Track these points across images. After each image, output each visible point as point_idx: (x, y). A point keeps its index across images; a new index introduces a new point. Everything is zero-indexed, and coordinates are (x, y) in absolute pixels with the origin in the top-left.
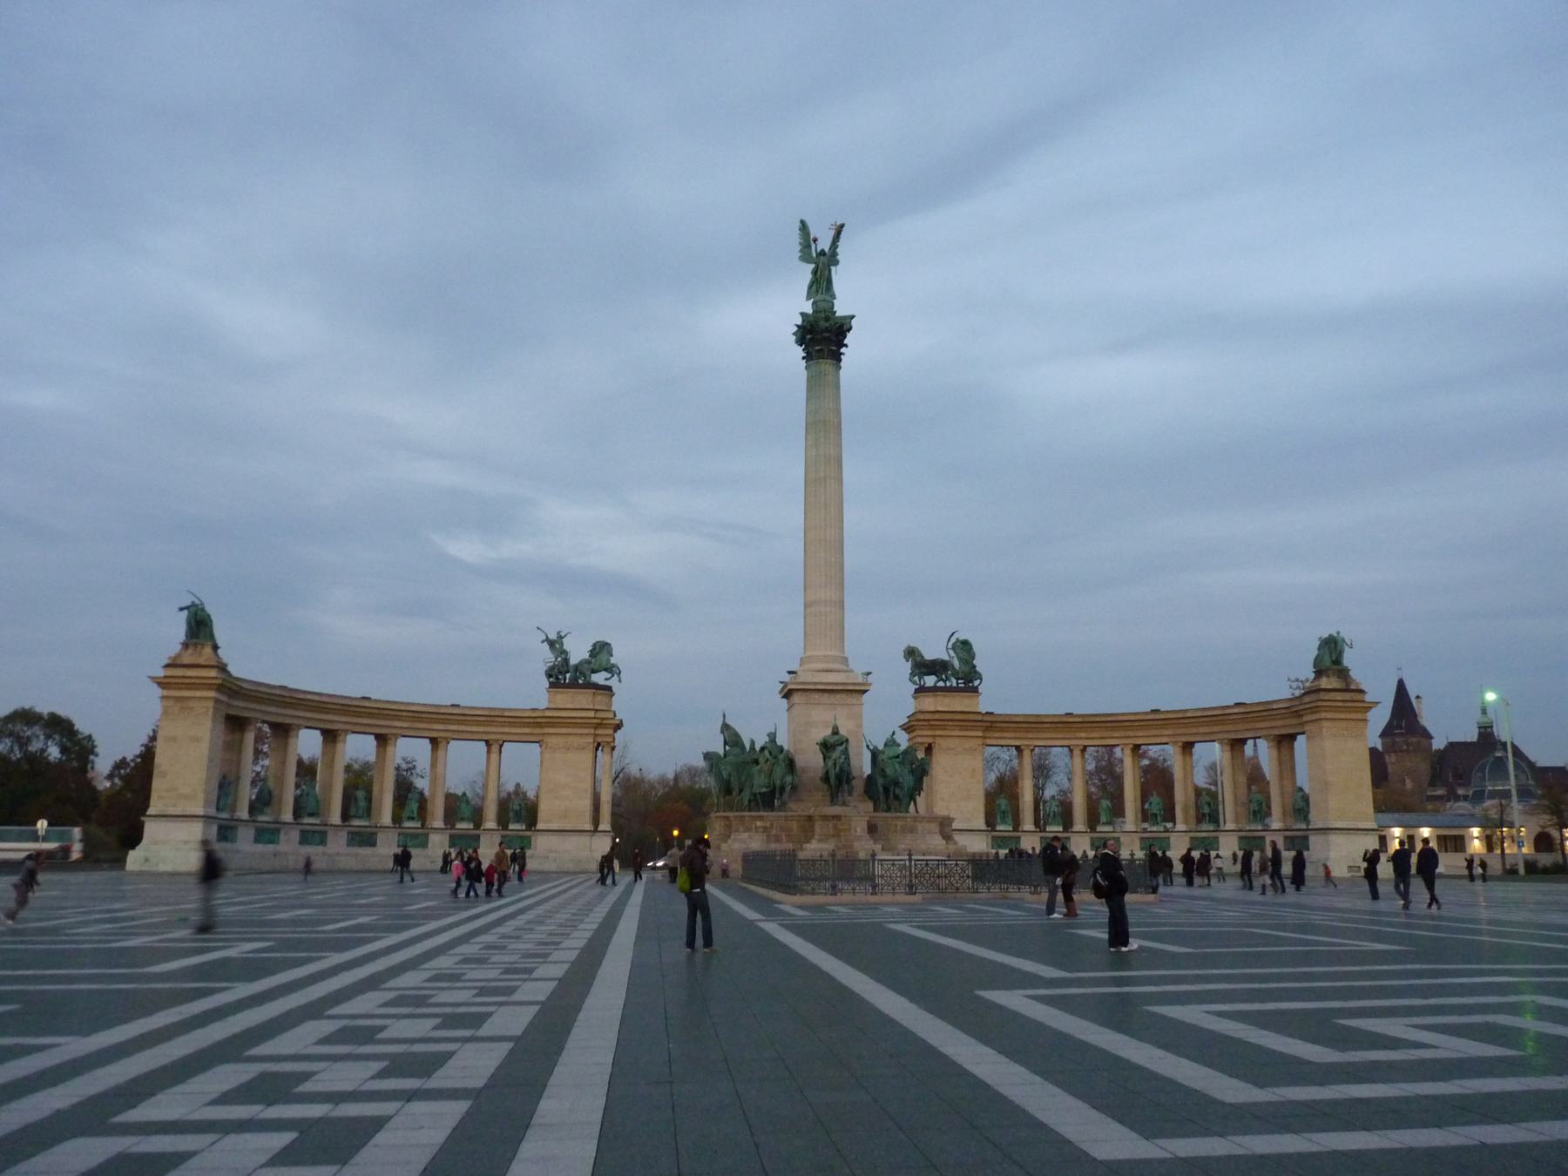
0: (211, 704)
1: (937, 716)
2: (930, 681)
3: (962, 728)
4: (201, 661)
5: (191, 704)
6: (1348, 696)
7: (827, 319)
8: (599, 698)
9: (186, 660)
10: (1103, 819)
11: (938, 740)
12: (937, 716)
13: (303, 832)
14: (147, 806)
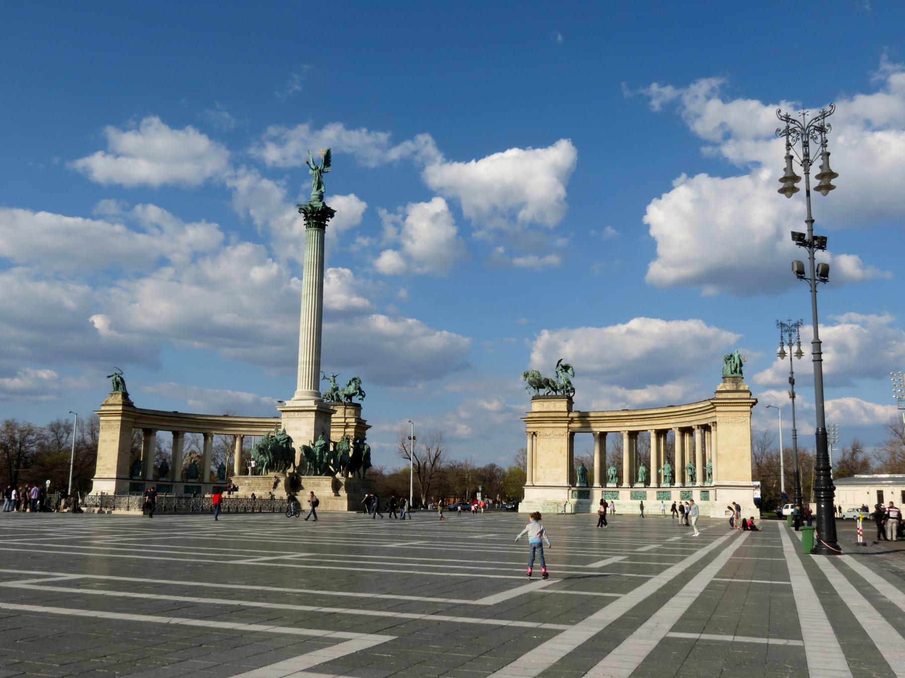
0: (119, 423)
1: (538, 415)
2: (542, 392)
3: (555, 422)
4: (116, 402)
5: (112, 423)
6: (737, 395)
7: (311, 206)
8: (347, 411)
9: (111, 402)
10: (640, 479)
11: (539, 430)
12: (538, 415)
13: (186, 487)
14: (94, 474)
